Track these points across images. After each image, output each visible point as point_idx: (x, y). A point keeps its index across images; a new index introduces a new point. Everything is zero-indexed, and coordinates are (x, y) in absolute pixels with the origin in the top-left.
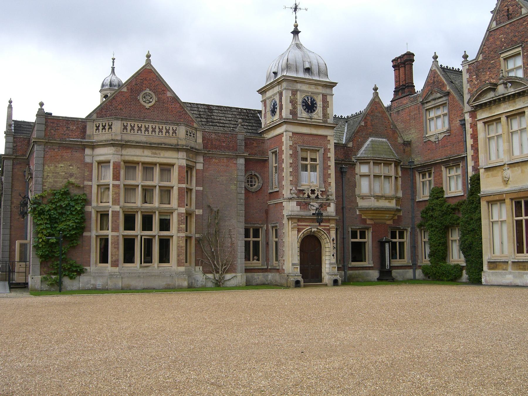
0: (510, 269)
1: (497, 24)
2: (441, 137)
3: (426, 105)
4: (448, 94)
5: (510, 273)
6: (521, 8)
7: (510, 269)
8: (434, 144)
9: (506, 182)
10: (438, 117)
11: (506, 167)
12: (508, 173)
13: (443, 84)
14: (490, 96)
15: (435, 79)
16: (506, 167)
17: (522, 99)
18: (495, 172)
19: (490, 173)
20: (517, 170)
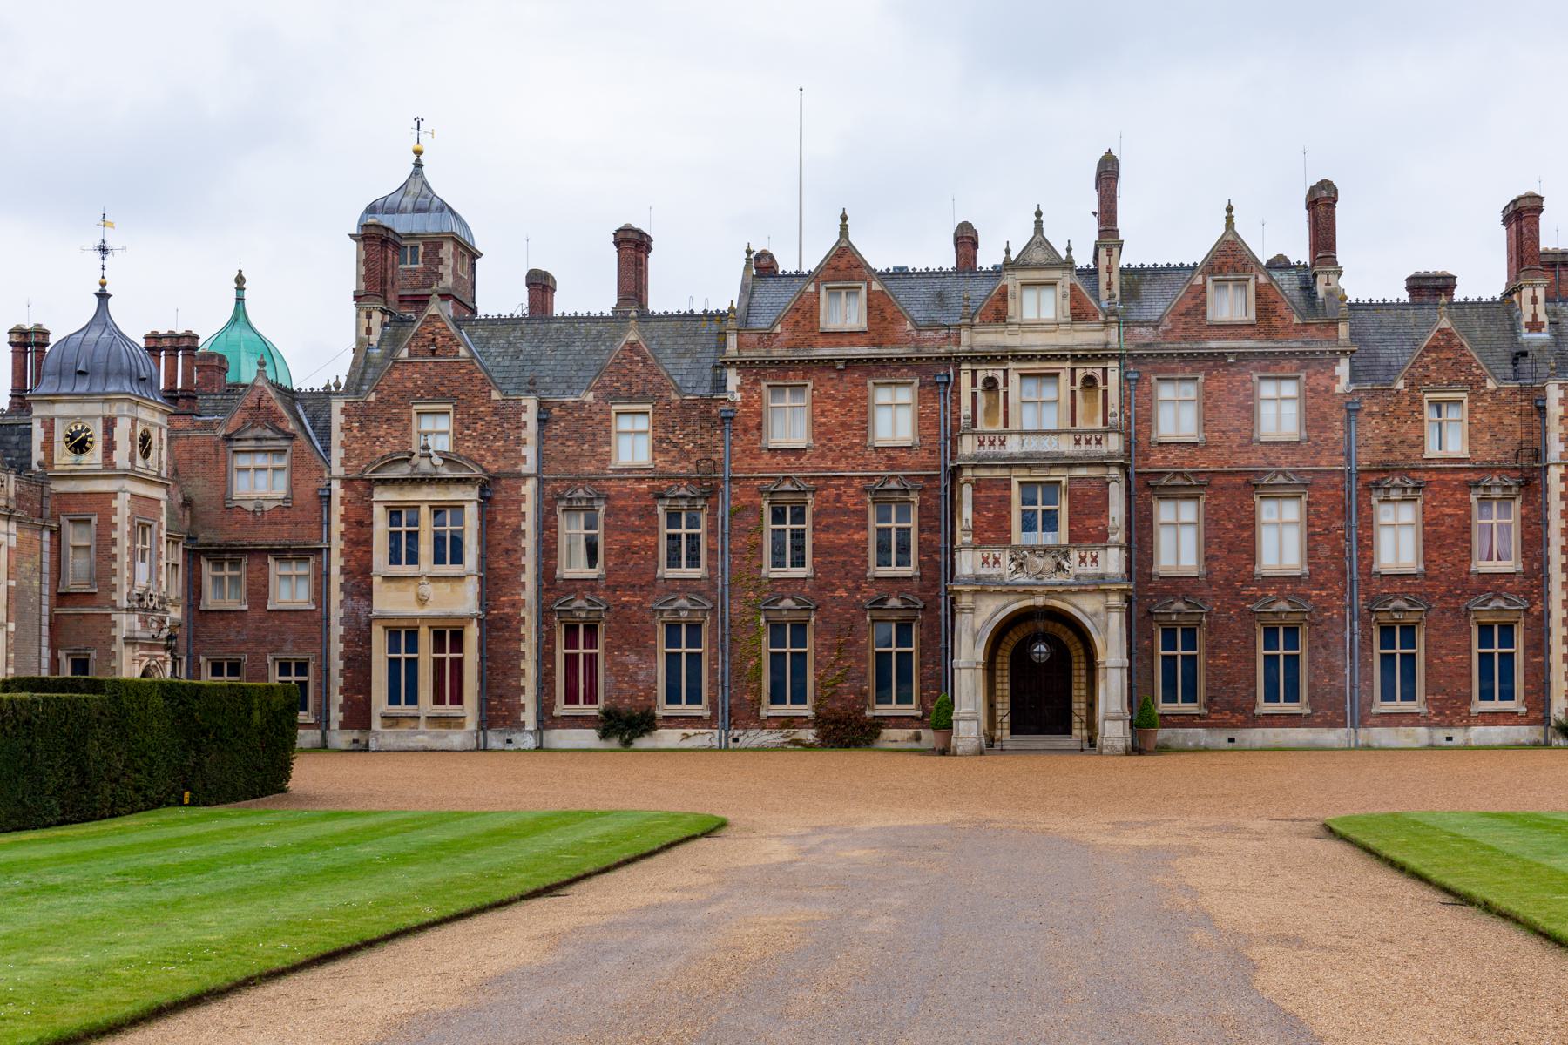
0: (422, 726)
1: (410, 356)
2: (268, 506)
3: (235, 444)
4: (291, 437)
5: (423, 733)
6: (458, 345)
7: (422, 726)
8: (250, 517)
9: (422, 601)
10: (265, 469)
11: (424, 580)
12: (428, 589)
13: (281, 417)
14: (403, 471)
15: (263, 404)
16: (424, 580)
17: (462, 487)
18: (402, 585)
19: (393, 585)
20: (445, 588)
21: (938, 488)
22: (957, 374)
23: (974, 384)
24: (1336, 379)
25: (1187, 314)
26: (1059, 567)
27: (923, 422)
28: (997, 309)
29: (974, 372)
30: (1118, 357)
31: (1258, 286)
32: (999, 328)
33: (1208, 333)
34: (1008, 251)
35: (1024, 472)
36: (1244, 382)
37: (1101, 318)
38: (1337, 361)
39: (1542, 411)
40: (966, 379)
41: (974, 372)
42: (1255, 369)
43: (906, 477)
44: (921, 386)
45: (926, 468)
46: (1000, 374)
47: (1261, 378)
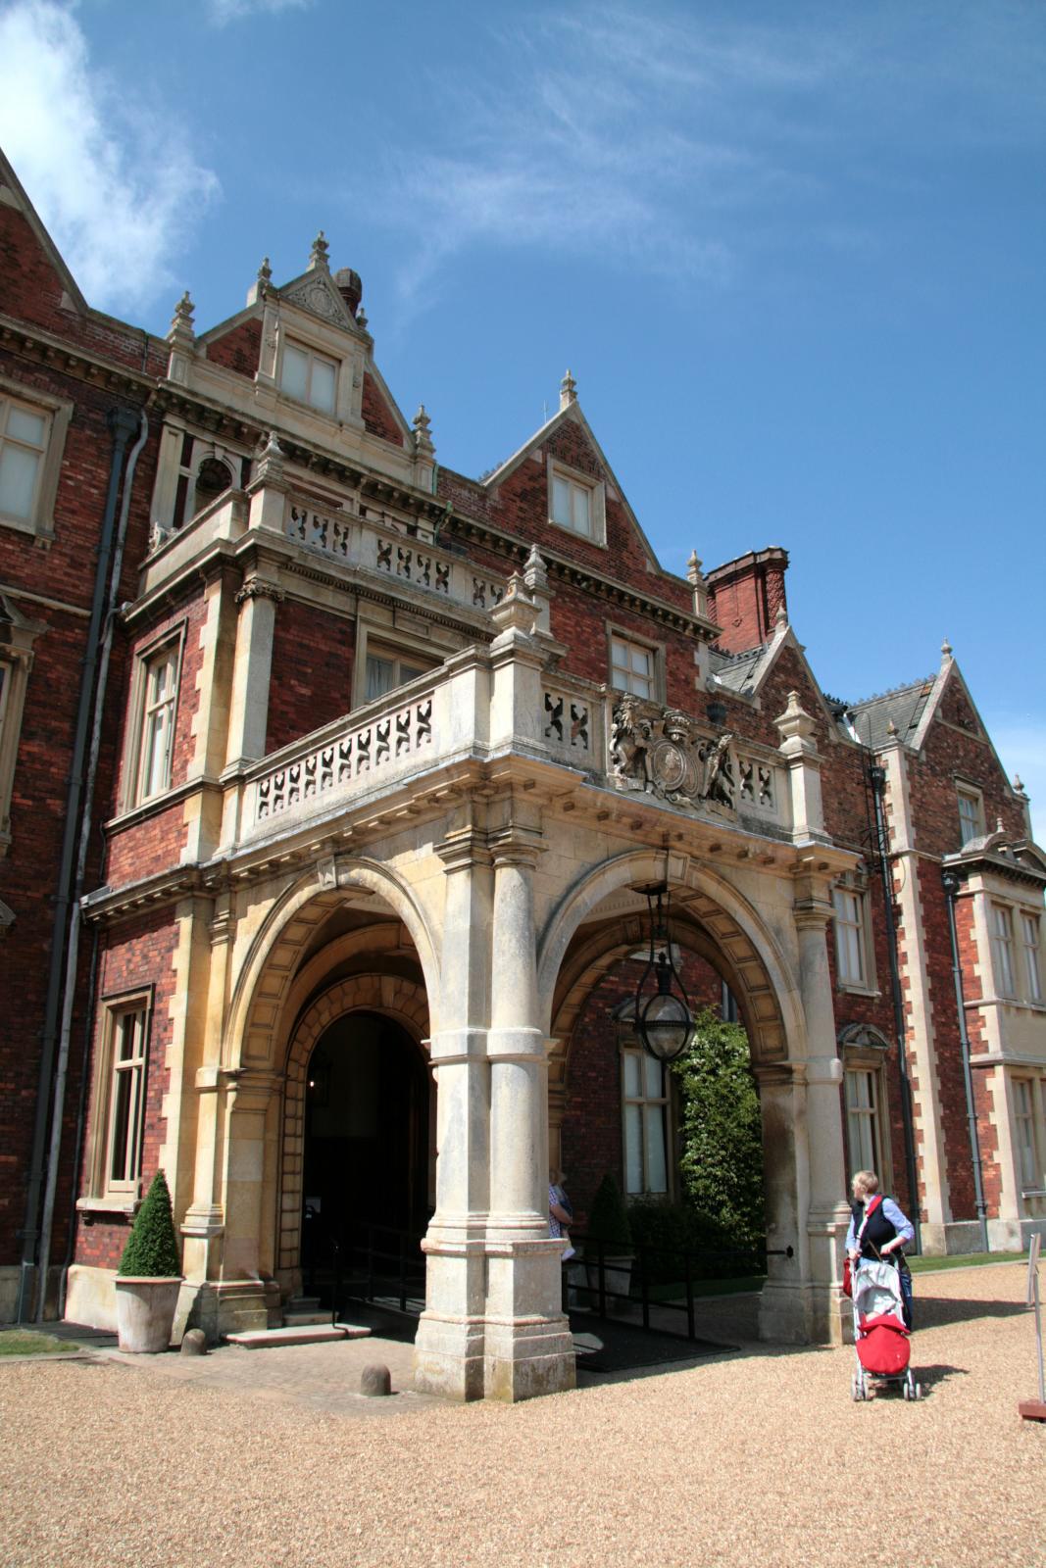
21: (80, 647)
22: (156, 434)
23: (186, 461)
24: (694, 667)
25: (523, 496)
26: (717, 794)
27: (64, 496)
28: (239, 352)
29: (189, 443)
30: (434, 514)
31: (608, 500)
32: (237, 381)
33: (549, 538)
34: (266, 272)
35: (382, 616)
36: (595, 631)
37: (407, 446)
38: (696, 642)
39: (878, 785)
40: (170, 447)
41: (189, 443)
42: (608, 616)
43: (10, 599)
44: (76, 422)
45: (58, 594)
46: (236, 466)
47: (615, 633)
